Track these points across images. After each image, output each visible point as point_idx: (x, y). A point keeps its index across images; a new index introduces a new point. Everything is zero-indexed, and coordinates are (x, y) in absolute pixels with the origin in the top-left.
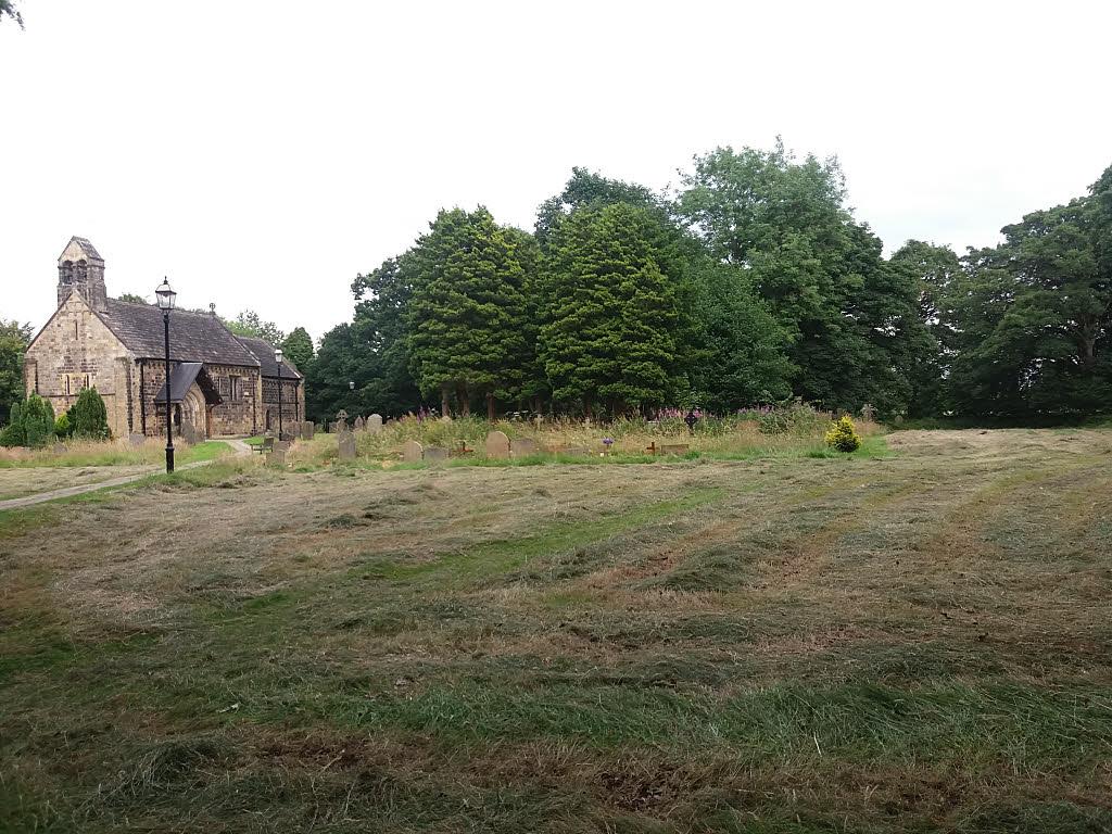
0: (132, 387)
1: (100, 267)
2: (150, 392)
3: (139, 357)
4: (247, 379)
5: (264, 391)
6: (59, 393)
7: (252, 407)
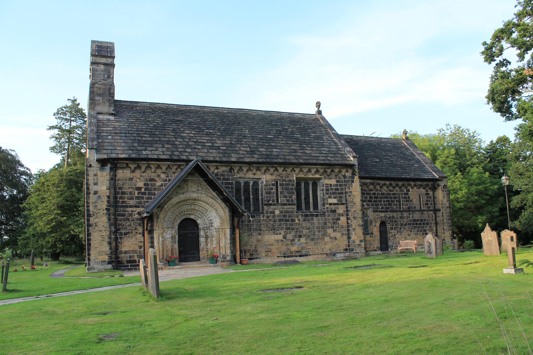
1: (105, 64)
2: (132, 202)
3: (105, 156)
4: (333, 182)
7: (343, 219)
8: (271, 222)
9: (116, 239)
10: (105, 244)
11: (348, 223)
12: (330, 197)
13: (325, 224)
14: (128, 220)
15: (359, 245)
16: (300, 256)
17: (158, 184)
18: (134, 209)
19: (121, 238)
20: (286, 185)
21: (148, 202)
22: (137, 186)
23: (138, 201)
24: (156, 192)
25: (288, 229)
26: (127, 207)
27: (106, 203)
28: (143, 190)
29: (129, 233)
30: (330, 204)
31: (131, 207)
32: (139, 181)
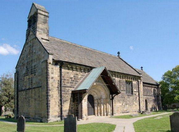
0: (50, 81)
2: (69, 85)
5: (144, 90)
6: (23, 89)
7: (138, 97)
8: (118, 98)
9: (61, 104)
10: (57, 106)
11: (139, 99)
12: (134, 89)
13: (133, 99)
14: (67, 94)
15: (143, 108)
16: (127, 112)
17: (80, 77)
18: (69, 88)
19: (63, 103)
20: (123, 82)
21: (75, 85)
22: (71, 77)
23: (71, 84)
24: (79, 81)
25: (123, 101)
26: (66, 87)
27: (57, 84)
28: (73, 79)
29: (67, 100)
30: (135, 92)
31: (68, 87)
32: (71, 74)
